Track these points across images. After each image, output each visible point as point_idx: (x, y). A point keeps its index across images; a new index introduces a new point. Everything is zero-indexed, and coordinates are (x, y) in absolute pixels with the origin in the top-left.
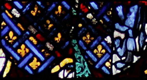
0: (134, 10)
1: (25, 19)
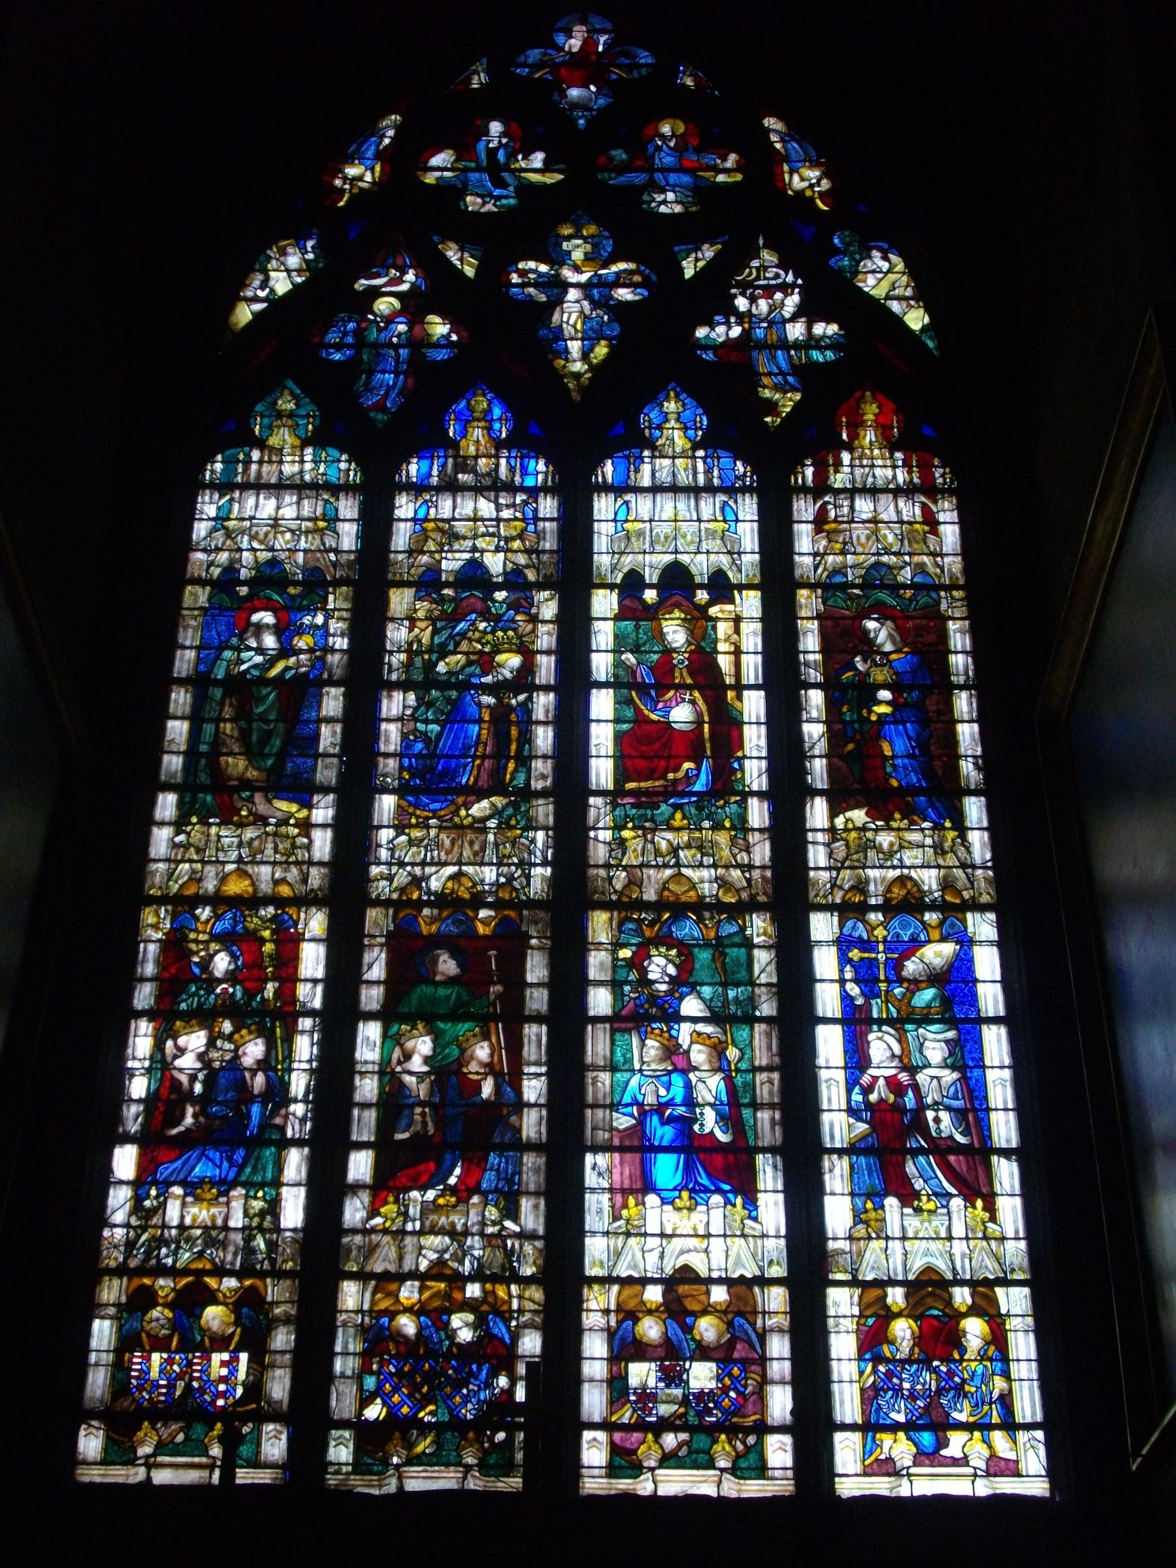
1: (399, 1373)
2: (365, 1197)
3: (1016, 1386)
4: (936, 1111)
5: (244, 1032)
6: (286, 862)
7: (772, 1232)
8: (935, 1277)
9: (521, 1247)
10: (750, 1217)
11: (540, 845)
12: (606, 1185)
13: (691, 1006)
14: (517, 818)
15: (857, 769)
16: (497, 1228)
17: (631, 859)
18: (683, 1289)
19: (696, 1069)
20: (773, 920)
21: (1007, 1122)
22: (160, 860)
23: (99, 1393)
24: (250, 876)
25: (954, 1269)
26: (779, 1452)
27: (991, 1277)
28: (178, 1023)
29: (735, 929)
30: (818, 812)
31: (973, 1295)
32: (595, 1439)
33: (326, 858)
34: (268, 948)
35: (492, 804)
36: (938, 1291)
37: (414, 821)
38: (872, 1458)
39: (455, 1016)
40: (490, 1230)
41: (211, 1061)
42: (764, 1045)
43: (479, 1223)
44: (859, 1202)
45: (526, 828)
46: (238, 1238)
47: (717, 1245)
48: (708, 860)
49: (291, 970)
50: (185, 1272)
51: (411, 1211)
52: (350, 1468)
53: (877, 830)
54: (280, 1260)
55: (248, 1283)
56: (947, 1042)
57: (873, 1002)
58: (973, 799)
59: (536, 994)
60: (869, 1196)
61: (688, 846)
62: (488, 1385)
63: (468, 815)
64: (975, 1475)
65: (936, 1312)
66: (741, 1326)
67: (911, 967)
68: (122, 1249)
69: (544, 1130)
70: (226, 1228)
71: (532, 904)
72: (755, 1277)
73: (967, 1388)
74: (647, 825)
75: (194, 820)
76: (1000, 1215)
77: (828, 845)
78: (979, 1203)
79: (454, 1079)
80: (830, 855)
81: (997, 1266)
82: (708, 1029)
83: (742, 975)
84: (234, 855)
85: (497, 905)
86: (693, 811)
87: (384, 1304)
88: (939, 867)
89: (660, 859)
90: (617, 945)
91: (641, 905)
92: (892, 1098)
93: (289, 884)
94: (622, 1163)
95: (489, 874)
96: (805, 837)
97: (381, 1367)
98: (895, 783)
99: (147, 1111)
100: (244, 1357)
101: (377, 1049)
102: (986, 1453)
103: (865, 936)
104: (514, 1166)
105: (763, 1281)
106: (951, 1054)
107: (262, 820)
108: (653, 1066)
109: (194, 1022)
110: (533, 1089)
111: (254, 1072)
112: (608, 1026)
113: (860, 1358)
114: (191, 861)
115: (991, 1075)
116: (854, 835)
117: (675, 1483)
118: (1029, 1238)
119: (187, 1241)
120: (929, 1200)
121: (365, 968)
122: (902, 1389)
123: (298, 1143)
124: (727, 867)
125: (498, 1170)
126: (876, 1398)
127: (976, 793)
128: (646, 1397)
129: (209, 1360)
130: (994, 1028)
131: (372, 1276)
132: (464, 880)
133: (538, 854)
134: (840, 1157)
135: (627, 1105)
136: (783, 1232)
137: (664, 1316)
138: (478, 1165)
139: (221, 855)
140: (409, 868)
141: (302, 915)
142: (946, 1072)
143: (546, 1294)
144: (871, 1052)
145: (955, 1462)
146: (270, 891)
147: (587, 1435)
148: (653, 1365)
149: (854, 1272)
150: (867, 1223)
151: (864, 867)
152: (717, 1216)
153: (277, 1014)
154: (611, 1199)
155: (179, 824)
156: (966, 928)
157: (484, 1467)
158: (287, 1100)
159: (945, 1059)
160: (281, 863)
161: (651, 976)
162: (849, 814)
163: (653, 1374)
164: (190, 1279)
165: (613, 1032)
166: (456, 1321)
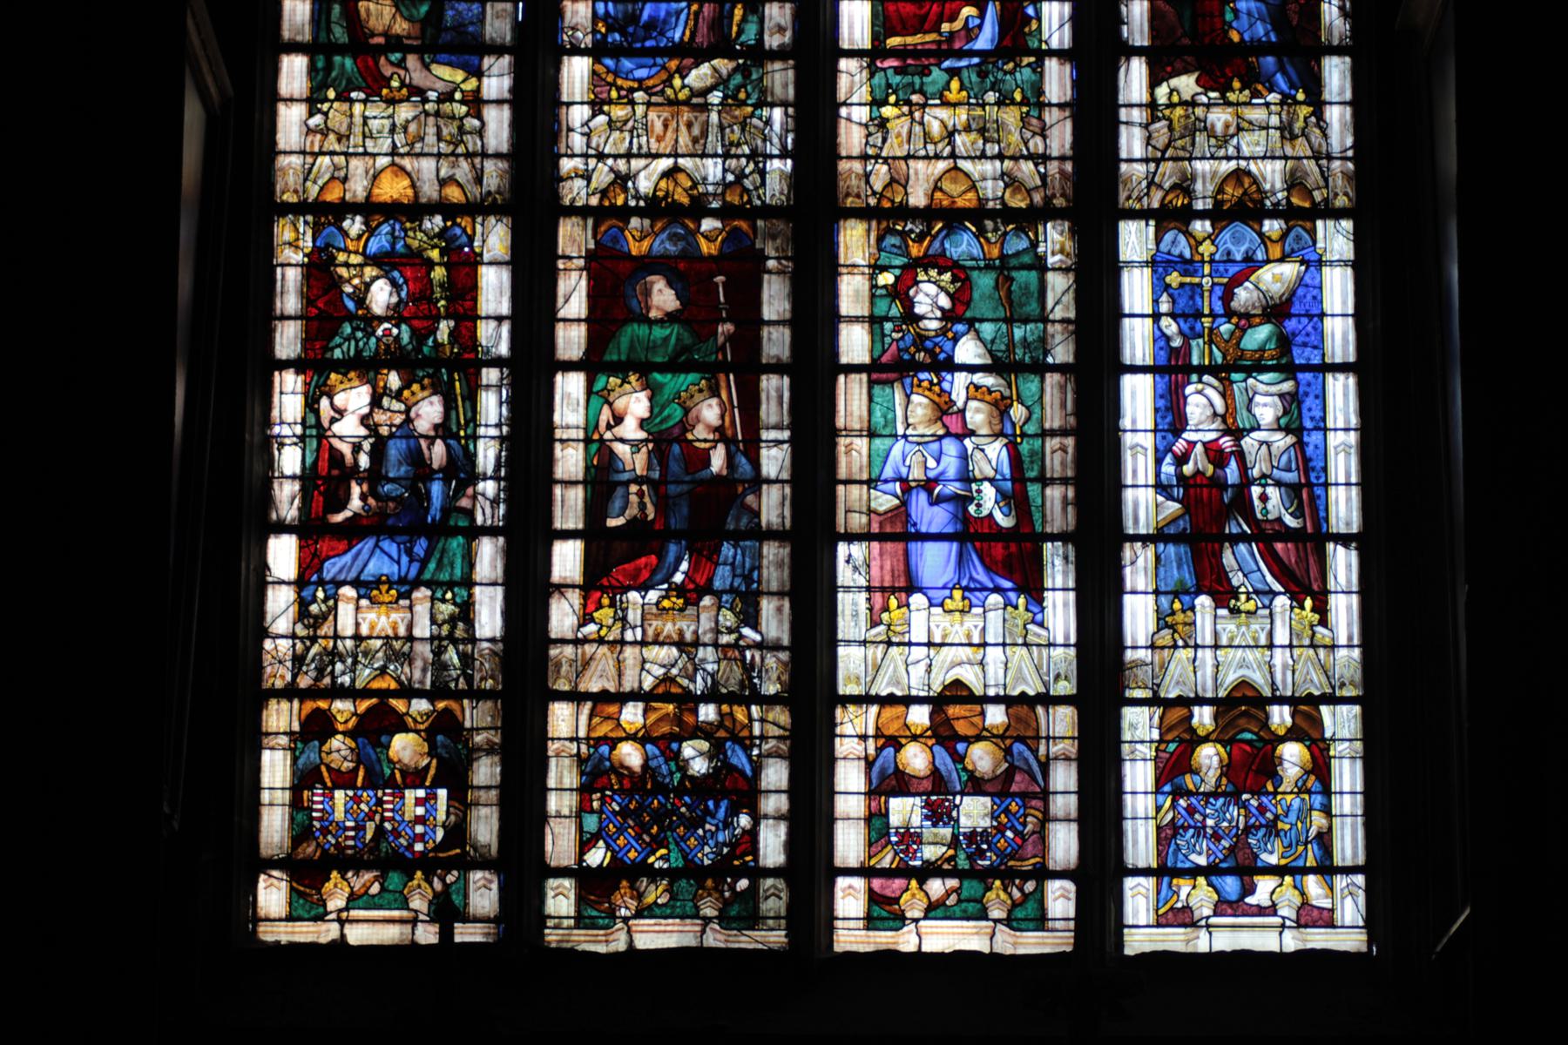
0: (724, 804)
1: (624, 813)
2: (575, 597)
3: (1336, 822)
4: (1264, 486)
5: (415, 387)
6: (453, 154)
7: (1060, 640)
8: (1250, 693)
9: (763, 659)
10: (1033, 622)
11: (777, 127)
12: (863, 583)
13: (967, 351)
14: (743, 94)
15: (1187, 14)
16: (734, 636)
17: (894, 148)
18: (953, 710)
19: (972, 433)
20: (1072, 232)
21: (1348, 499)
22: (291, 153)
23: (276, 838)
24: (408, 174)
25: (1273, 683)
26: (1060, 900)
27: (1316, 693)
28: (333, 376)
29: (1023, 244)
30: (1134, 79)
31: (1293, 716)
32: (850, 887)
33: (505, 148)
34: (439, 273)
35: (715, 69)
36: (1253, 711)
37: (614, 94)
38: (1168, 907)
39: (674, 366)
40: (725, 639)
41: (377, 425)
42: (1057, 402)
43: (711, 630)
44: (1164, 600)
45: (760, 104)
46: (424, 650)
47: (995, 655)
48: (993, 149)
49: (468, 304)
50: (366, 693)
51: (630, 617)
52: (572, 922)
53: (1208, 106)
54: (477, 677)
55: (441, 705)
56: (1281, 396)
57: (1193, 343)
58: (1335, 60)
59: (775, 335)
60: (1176, 594)
61: (968, 129)
62: (727, 824)
63: (684, 86)
64: (1283, 926)
65: (1248, 736)
66: (1020, 753)
67: (1244, 296)
68: (289, 664)
69: (787, 513)
70: (410, 638)
71: (767, 211)
72: (1038, 694)
73: (1280, 825)
74: (915, 98)
75: (331, 94)
76: (1332, 617)
77: (1146, 126)
78: (1308, 603)
79: (676, 448)
80: (1148, 141)
81: (1323, 679)
82: (988, 380)
83: (1033, 308)
84: (385, 145)
85: (724, 213)
86: (974, 78)
87: (603, 730)
88: (1286, 158)
89: (930, 147)
90: (877, 268)
91: (905, 212)
92: (1210, 470)
93: (459, 185)
94: (881, 554)
95: (713, 169)
96: (1116, 115)
97: (602, 804)
98: (1235, 37)
99: (305, 493)
100: (442, 793)
101: (582, 410)
102: (1298, 901)
103: (1187, 254)
104: (753, 558)
105: (1047, 700)
106: (1285, 413)
107: (419, 92)
108: (920, 431)
109: (352, 374)
110: (774, 461)
111: (431, 440)
112: (864, 377)
113: (1158, 791)
114: (332, 153)
115: (1334, 439)
116: (1179, 111)
117: (943, 937)
118: (1365, 645)
119: (365, 654)
120: (1248, 599)
121: (560, 300)
122: (1204, 827)
123: (491, 531)
124: (1014, 158)
125: (733, 565)
126: (1174, 836)
127: (1338, 51)
128: (910, 838)
129: (403, 797)
130: (1341, 377)
131: (587, 696)
132: (681, 178)
133: (776, 140)
134: (1144, 546)
135: (886, 481)
136: (1073, 640)
137: (930, 742)
138: (709, 559)
139: (369, 143)
140: (610, 162)
141: (479, 228)
142: (1278, 436)
143: (793, 716)
144: (1189, 409)
145: (1261, 911)
146: (435, 195)
147: (842, 882)
148: (918, 800)
149: (1156, 688)
150: (1172, 627)
151: (1190, 159)
152: (995, 618)
153: (454, 364)
154: (869, 600)
155: (313, 101)
156: (1315, 242)
157: (724, 920)
158: (474, 477)
159: (1278, 419)
160: (447, 155)
161: (918, 310)
162: (1174, 82)
163: (918, 811)
164: (374, 701)
165: (871, 384)
166: (688, 750)
